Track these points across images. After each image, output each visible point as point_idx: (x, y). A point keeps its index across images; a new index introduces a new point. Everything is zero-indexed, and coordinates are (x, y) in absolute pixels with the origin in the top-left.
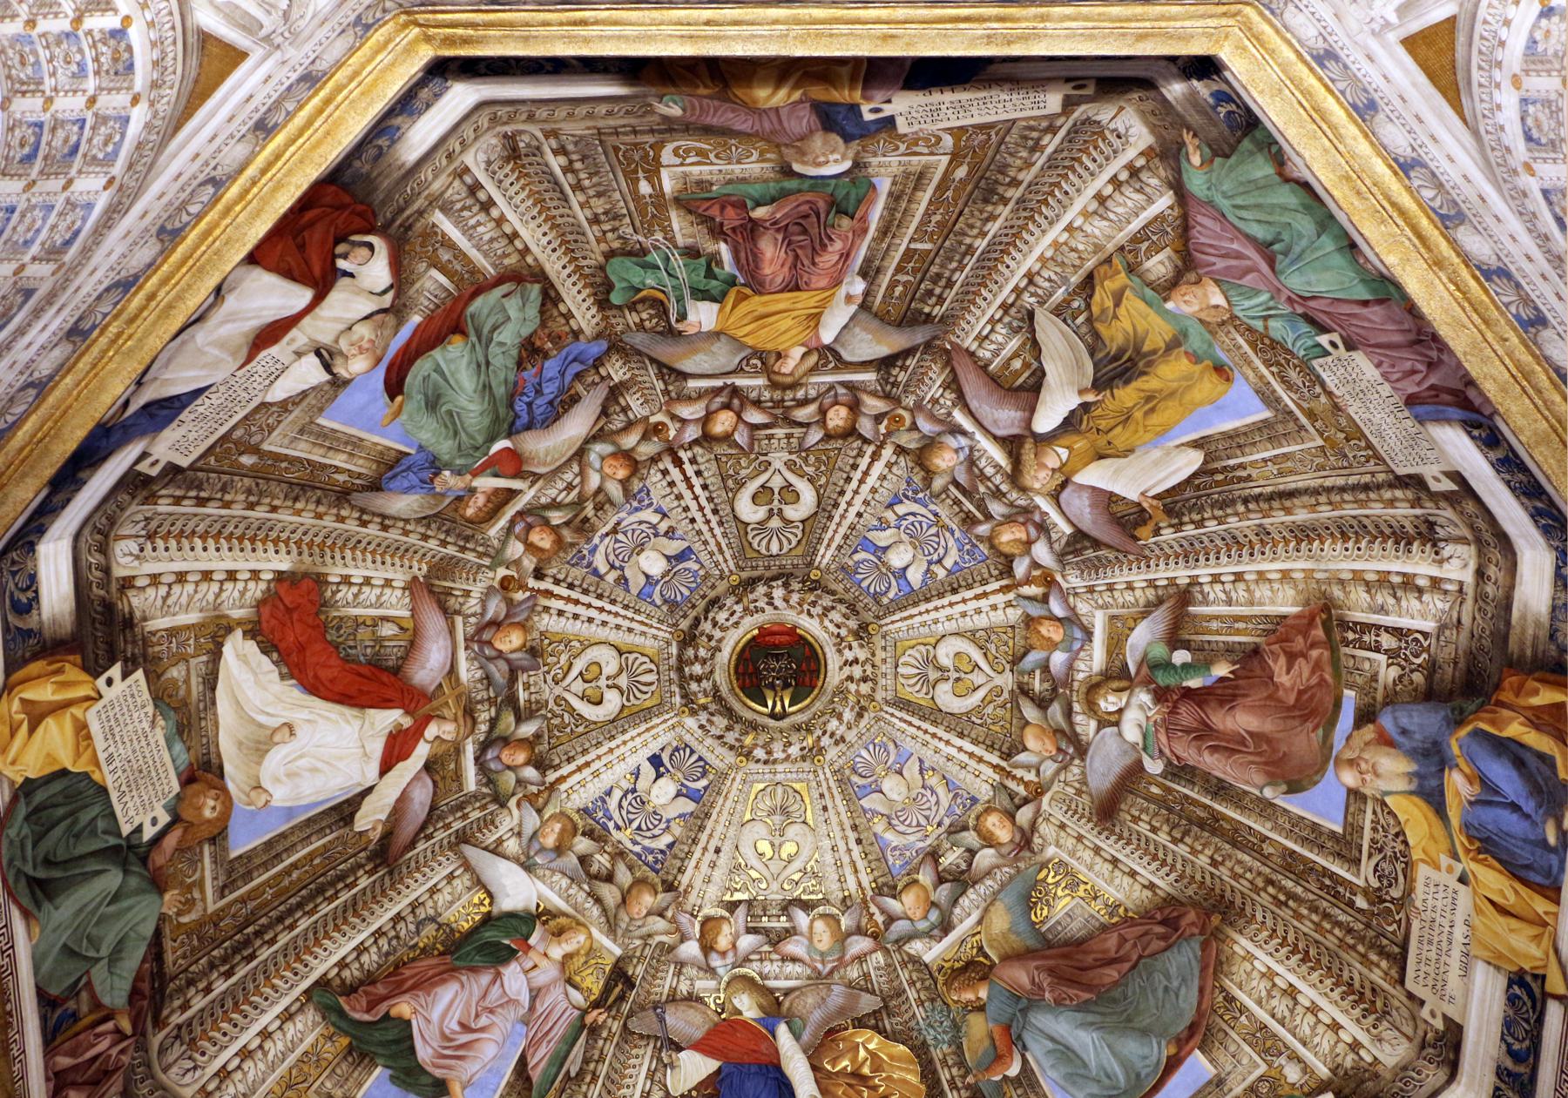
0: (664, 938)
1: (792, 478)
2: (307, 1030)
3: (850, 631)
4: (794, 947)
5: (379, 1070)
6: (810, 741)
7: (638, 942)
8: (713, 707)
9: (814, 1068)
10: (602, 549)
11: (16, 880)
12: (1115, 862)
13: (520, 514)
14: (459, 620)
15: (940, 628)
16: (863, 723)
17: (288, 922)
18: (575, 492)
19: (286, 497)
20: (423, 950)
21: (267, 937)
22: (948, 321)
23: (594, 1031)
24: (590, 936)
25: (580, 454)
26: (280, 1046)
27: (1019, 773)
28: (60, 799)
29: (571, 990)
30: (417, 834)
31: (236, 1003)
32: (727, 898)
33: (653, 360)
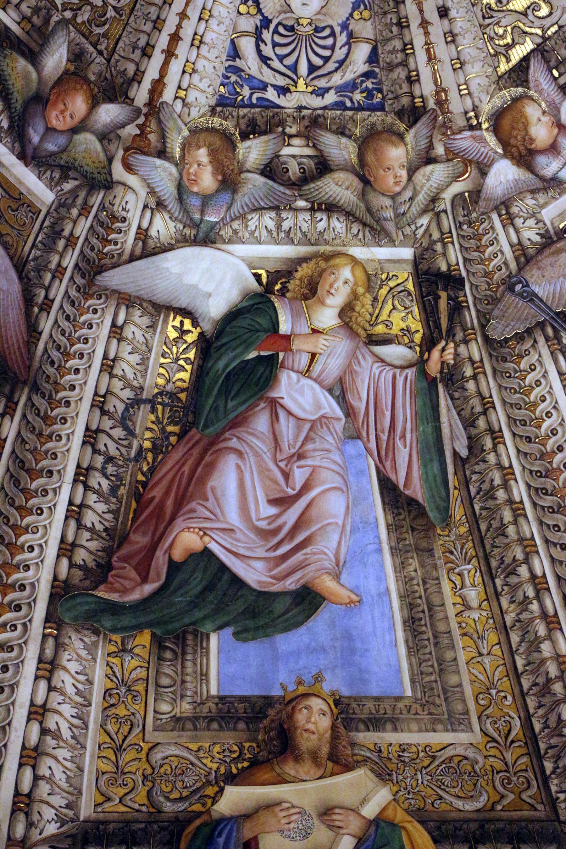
0: (457, 188)
5: (214, 640)
7: (424, 221)
20: (155, 449)
24: (355, 262)
26: (67, 710)
30: (28, 313)
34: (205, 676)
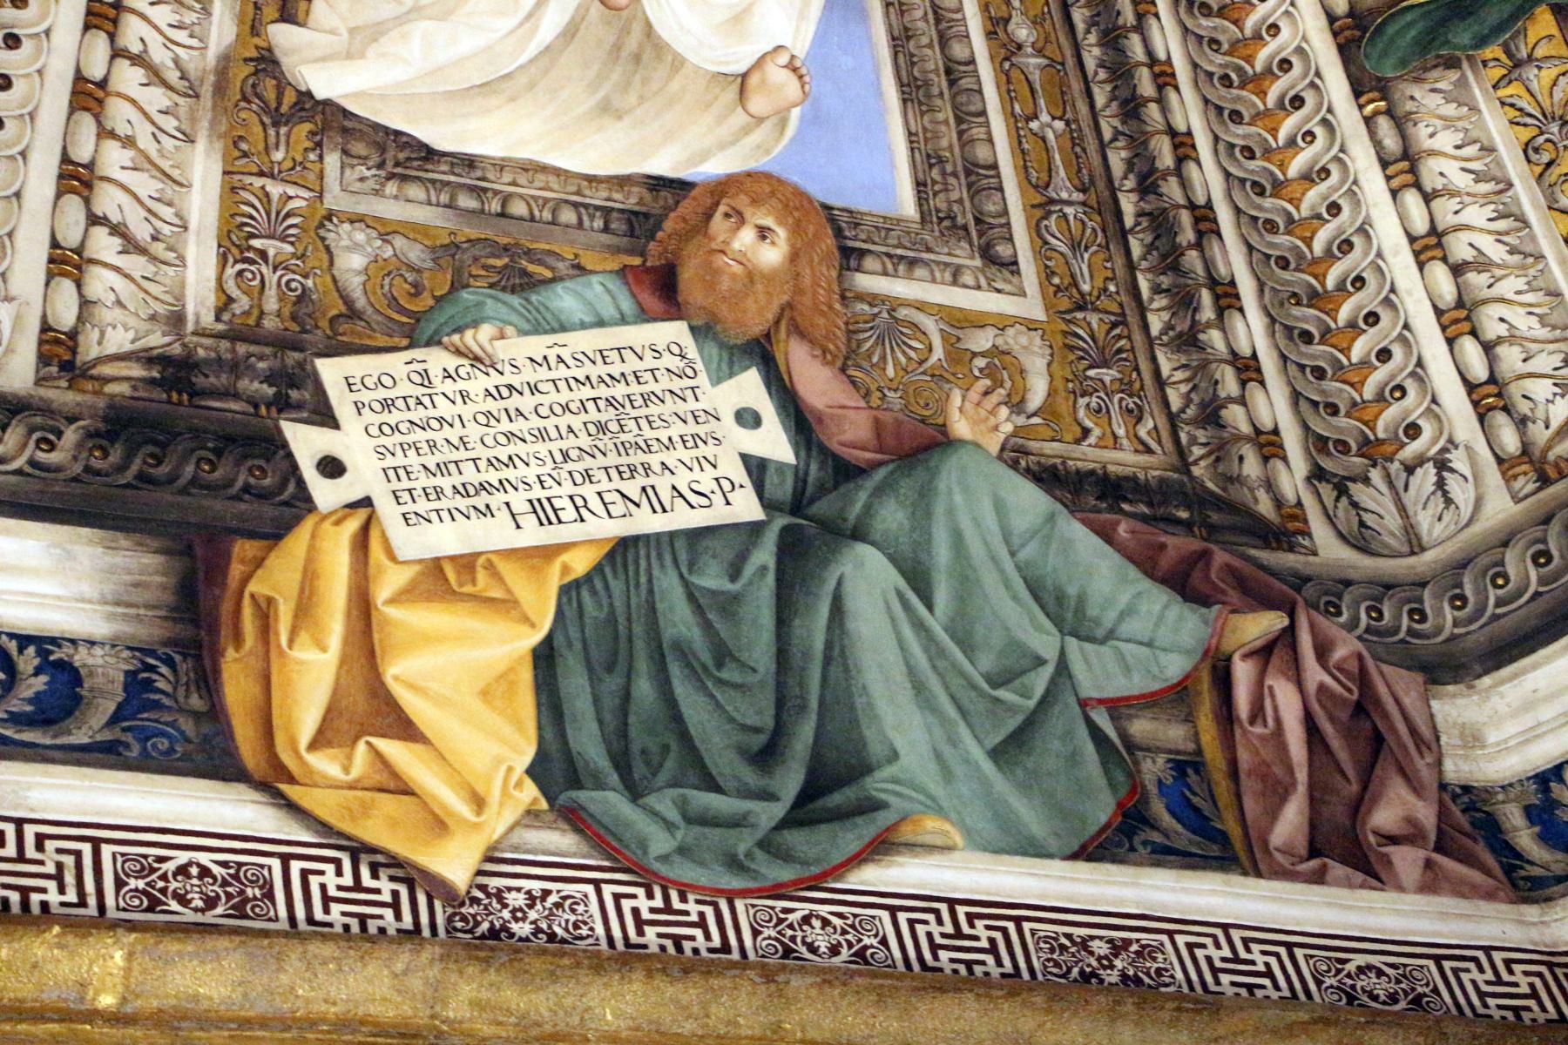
11: (786, 857)
17: (1146, 87)
21: (1166, 160)
26: (1476, 215)
28: (612, 683)
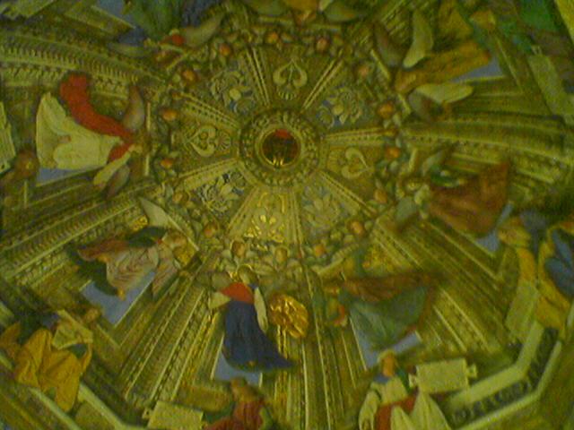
1: (299, 69)
2: (62, 261)
3: (312, 138)
4: (268, 259)
5: (89, 281)
6: (288, 179)
8: (252, 158)
9: (267, 308)
10: (214, 85)
12: (400, 251)
13: (181, 64)
14: (149, 104)
15: (349, 143)
16: (311, 177)
17: (60, 217)
18: (205, 59)
19: (75, 39)
22: (376, 10)
23: (182, 279)
24: (187, 241)
25: (209, 42)
27: (370, 208)
29: (176, 262)
31: (32, 246)
32: (245, 235)
33: (247, 6)
34: (81, 285)
